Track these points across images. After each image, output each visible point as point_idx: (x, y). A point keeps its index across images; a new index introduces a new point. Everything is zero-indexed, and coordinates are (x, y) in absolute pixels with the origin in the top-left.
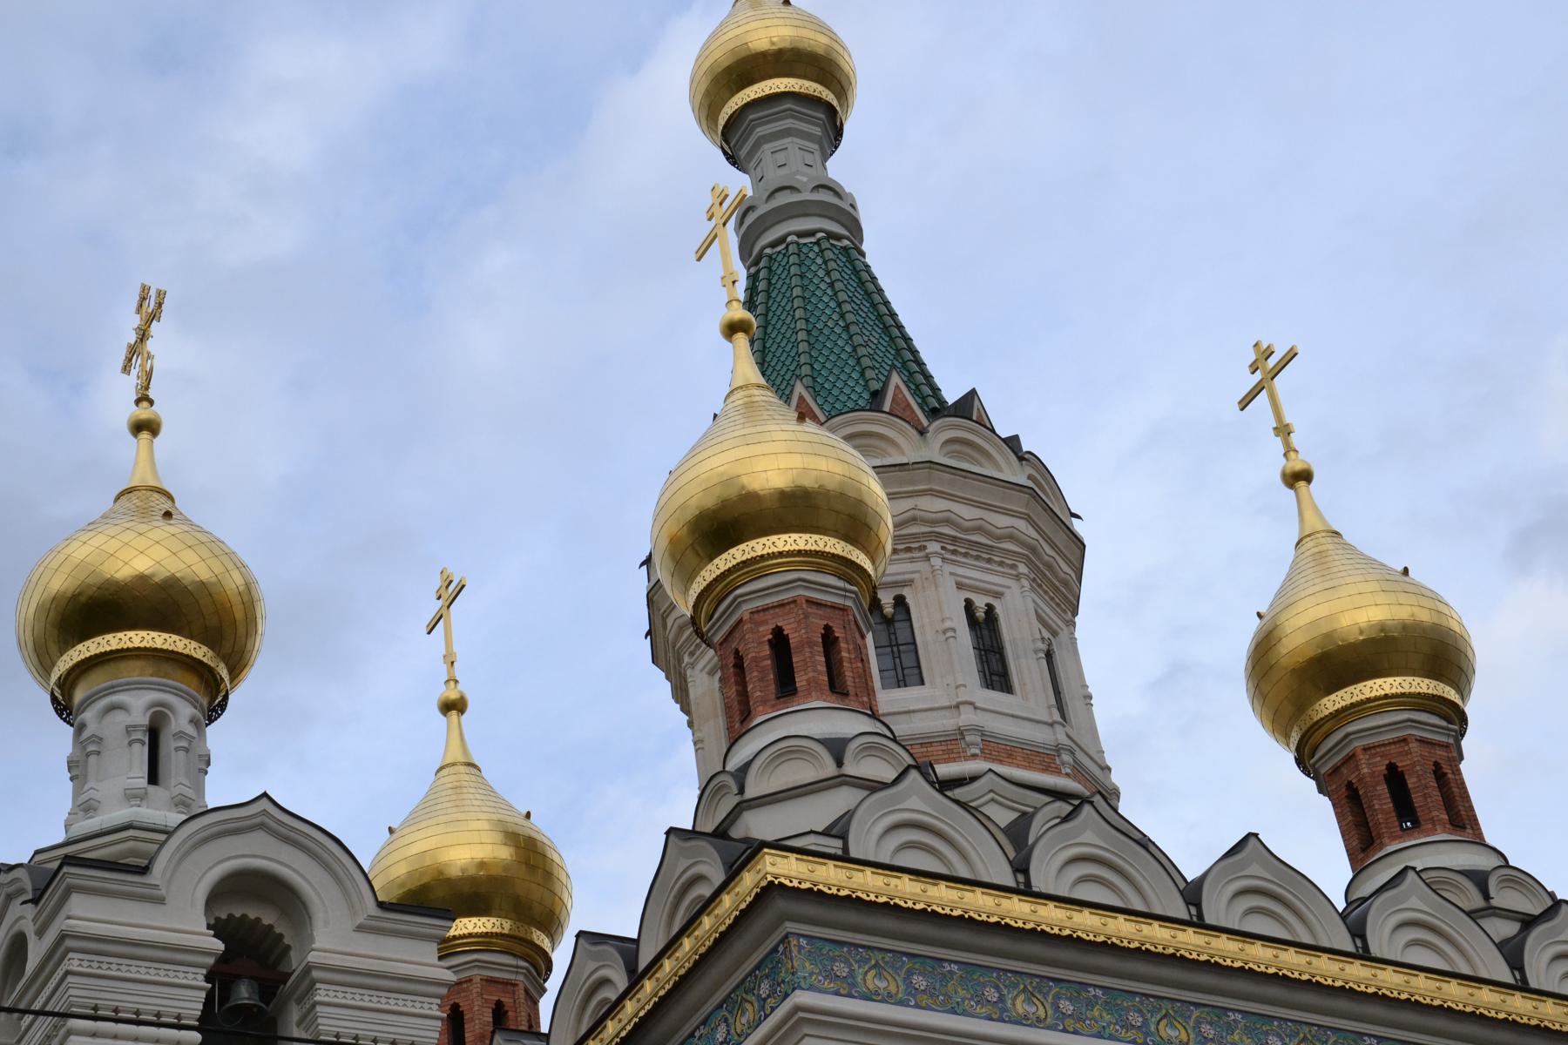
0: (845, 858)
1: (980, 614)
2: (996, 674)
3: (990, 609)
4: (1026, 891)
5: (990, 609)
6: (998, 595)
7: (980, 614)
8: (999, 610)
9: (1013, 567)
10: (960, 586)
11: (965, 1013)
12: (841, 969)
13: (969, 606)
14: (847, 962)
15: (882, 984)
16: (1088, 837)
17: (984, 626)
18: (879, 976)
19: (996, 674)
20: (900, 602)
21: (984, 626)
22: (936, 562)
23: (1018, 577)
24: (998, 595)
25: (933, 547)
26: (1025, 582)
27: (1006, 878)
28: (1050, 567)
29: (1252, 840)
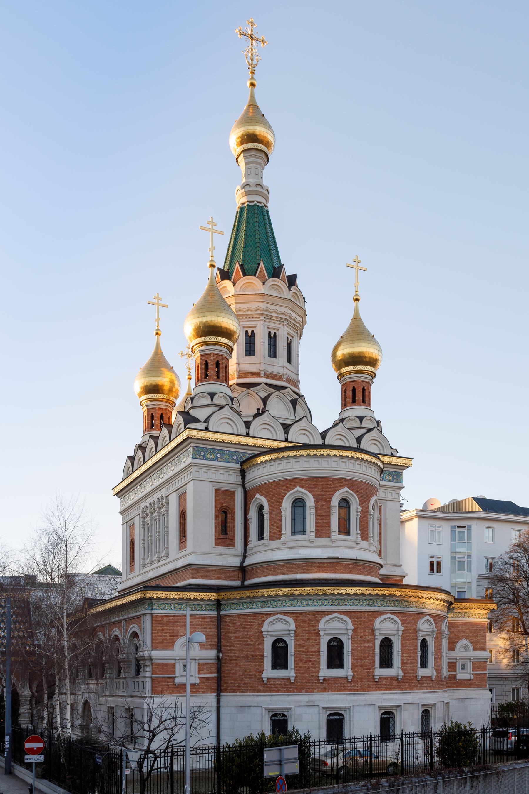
0: (207, 429)
1: (272, 336)
2: (273, 353)
3: (275, 333)
4: (248, 435)
5: (275, 333)
6: (278, 330)
7: (272, 336)
8: (277, 334)
9: (283, 322)
10: (268, 328)
11: (228, 462)
12: (202, 454)
13: (270, 332)
14: (204, 452)
15: (211, 457)
16: (267, 419)
17: (272, 339)
18: (210, 455)
19: (273, 353)
20: (253, 331)
21: (272, 339)
22: (262, 322)
23: (283, 325)
24: (278, 330)
25: (262, 318)
26: (285, 326)
27: (244, 431)
28: (294, 320)
29: (305, 418)
